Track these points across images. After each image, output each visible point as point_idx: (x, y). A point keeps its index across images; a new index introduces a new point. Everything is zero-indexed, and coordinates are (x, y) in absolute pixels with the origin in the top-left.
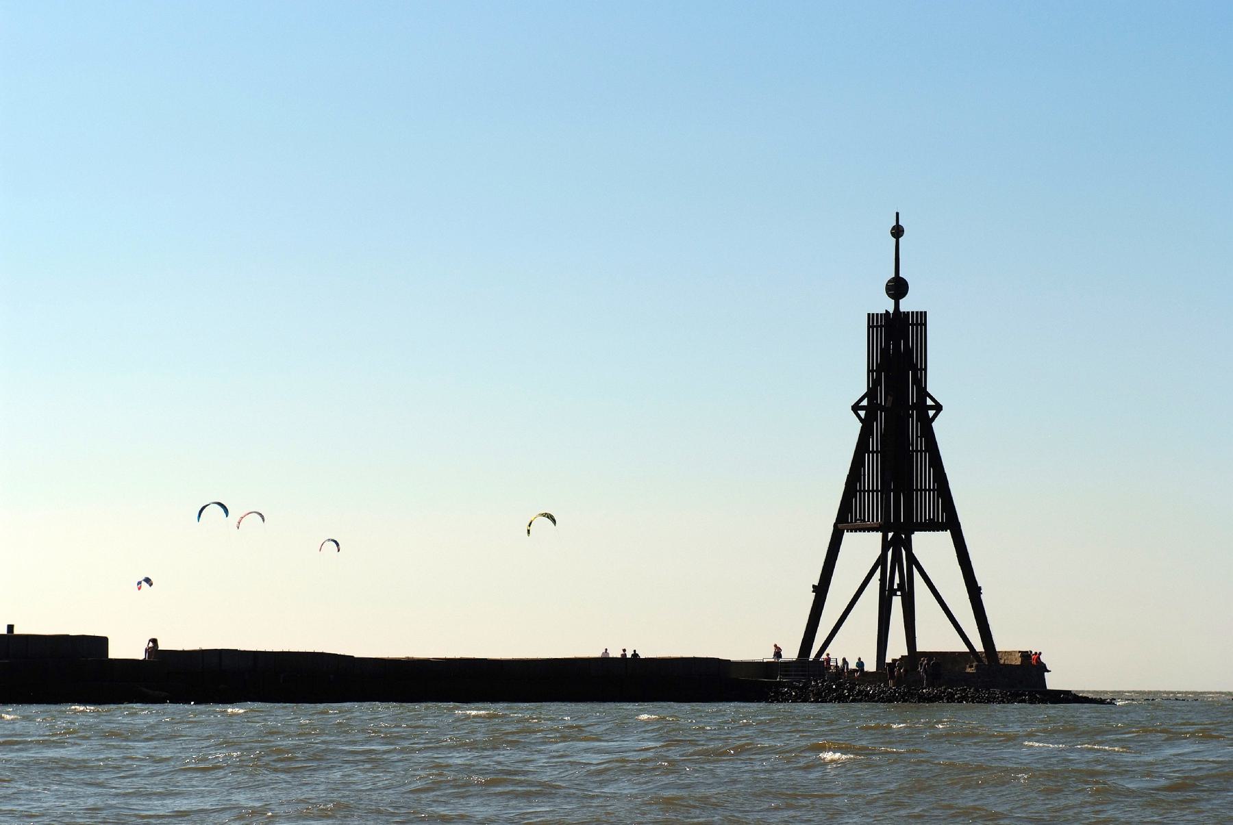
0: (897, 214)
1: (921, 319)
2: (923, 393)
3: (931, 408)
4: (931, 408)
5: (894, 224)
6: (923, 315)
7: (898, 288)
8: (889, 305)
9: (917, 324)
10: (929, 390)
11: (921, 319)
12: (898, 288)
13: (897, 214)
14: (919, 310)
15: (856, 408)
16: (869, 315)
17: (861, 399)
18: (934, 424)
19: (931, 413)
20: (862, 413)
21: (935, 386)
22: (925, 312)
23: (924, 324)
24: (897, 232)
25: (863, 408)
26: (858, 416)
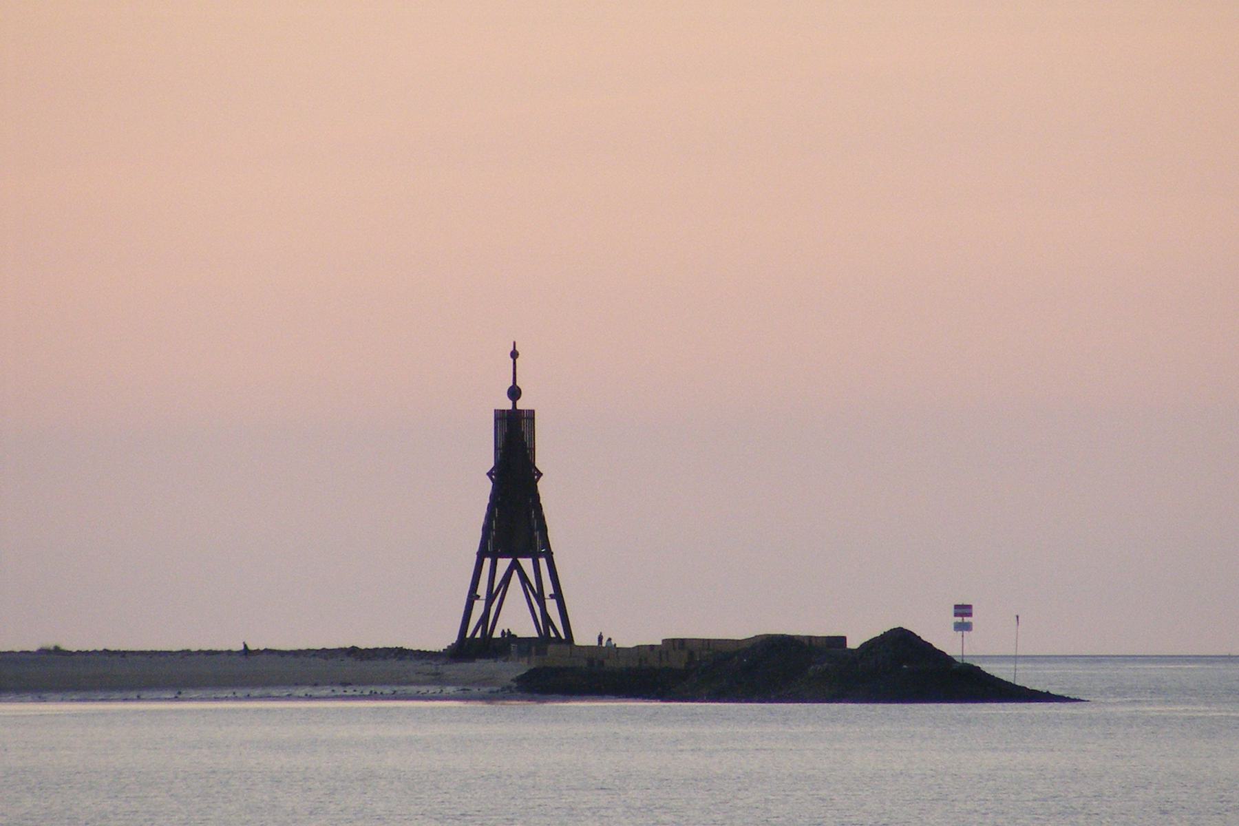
0: (514, 343)
5: (512, 349)
6: (533, 412)
7: (515, 393)
8: (507, 405)
10: (536, 465)
12: (515, 393)
13: (514, 343)
14: (530, 409)
16: (495, 410)
24: (514, 355)
26: (491, 479)
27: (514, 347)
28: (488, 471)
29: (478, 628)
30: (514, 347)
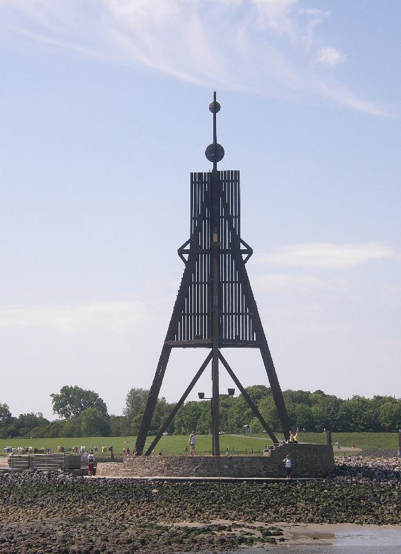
0: (215, 93)
1: (234, 177)
2: (236, 239)
3: (244, 252)
4: (244, 252)
6: (237, 173)
7: (215, 152)
8: (206, 167)
9: (232, 181)
10: (242, 237)
11: (234, 177)
12: (215, 152)
13: (215, 93)
15: (181, 252)
16: (192, 174)
18: (247, 265)
19: (244, 256)
20: (186, 256)
21: (247, 234)
22: (239, 171)
23: (237, 181)
24: (215, 108)
25: (186, 252)
26: (183, 259)
29: (218, 363)
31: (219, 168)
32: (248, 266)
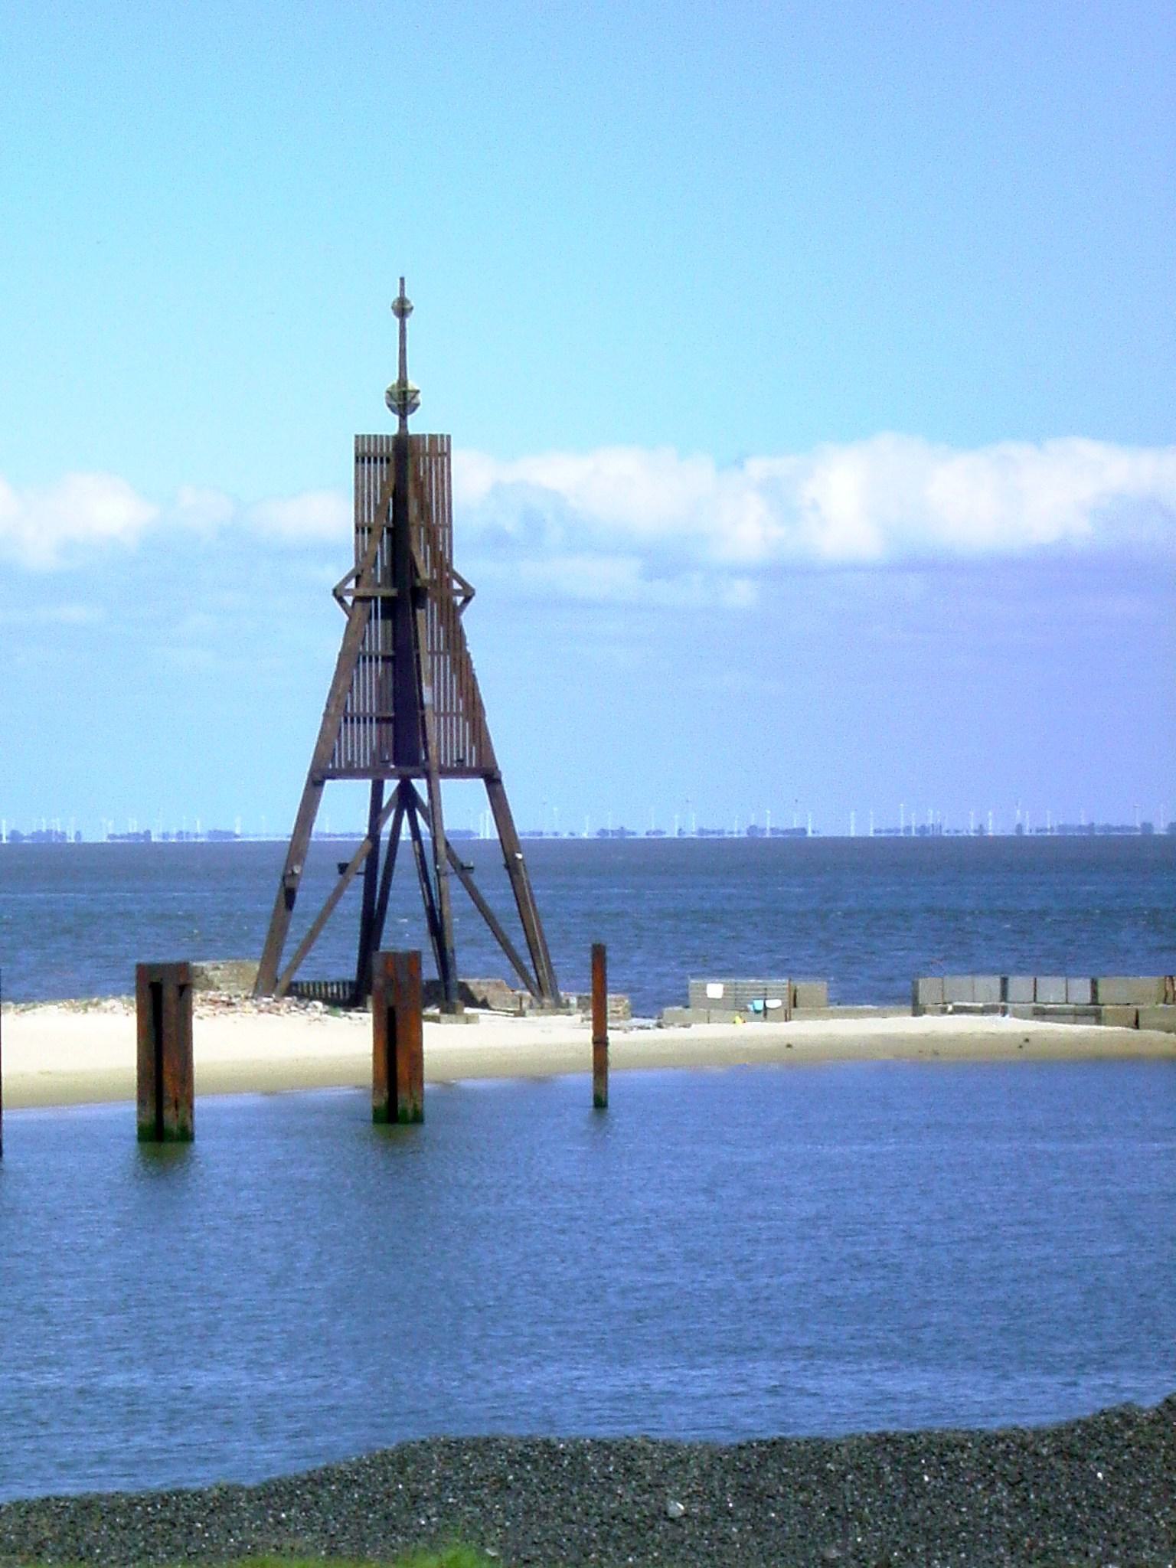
0: (402, 280)
3: (458, 593)
4: (458, 593)
7: (403, 401)
8: (388, 425)
10: (457, 567)
11: (439, 449)
12: (403, 401)
13: (402, 280)
16: (357, 437)
17: (347, 580)
20: (349, 600)
22: (449, 437)
24: (402, 310)
27: (402, 290)
28: (334, 586)
30: (402, 290)
31: (412, 430)
32: (467, 619)
